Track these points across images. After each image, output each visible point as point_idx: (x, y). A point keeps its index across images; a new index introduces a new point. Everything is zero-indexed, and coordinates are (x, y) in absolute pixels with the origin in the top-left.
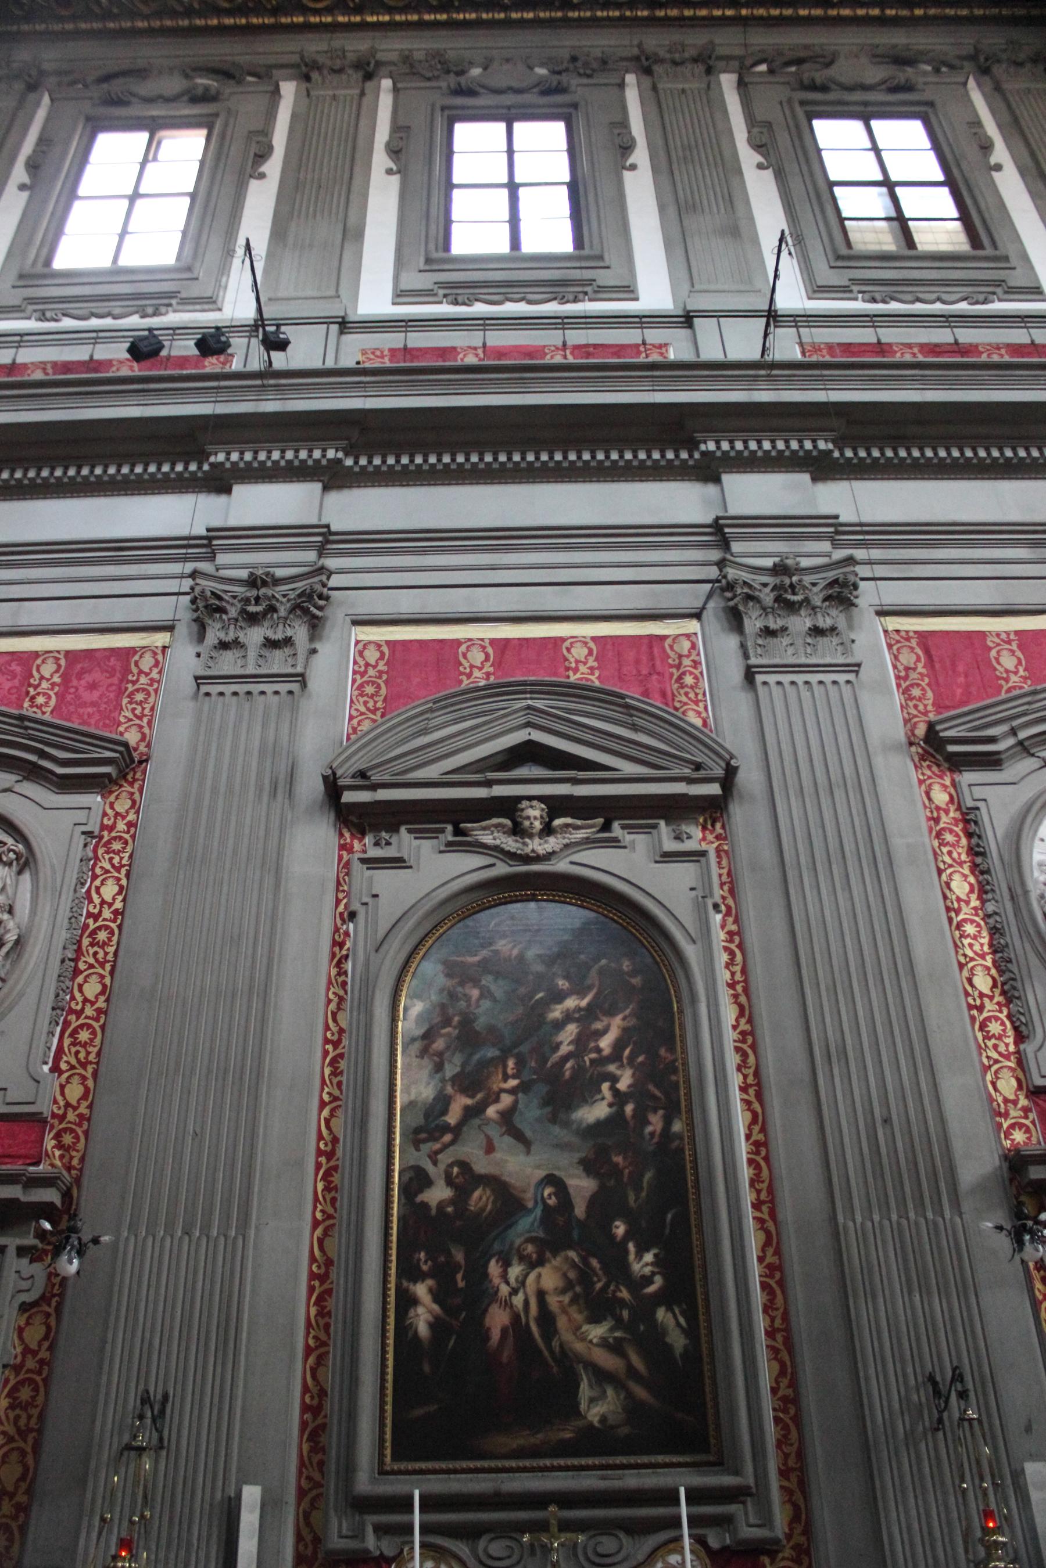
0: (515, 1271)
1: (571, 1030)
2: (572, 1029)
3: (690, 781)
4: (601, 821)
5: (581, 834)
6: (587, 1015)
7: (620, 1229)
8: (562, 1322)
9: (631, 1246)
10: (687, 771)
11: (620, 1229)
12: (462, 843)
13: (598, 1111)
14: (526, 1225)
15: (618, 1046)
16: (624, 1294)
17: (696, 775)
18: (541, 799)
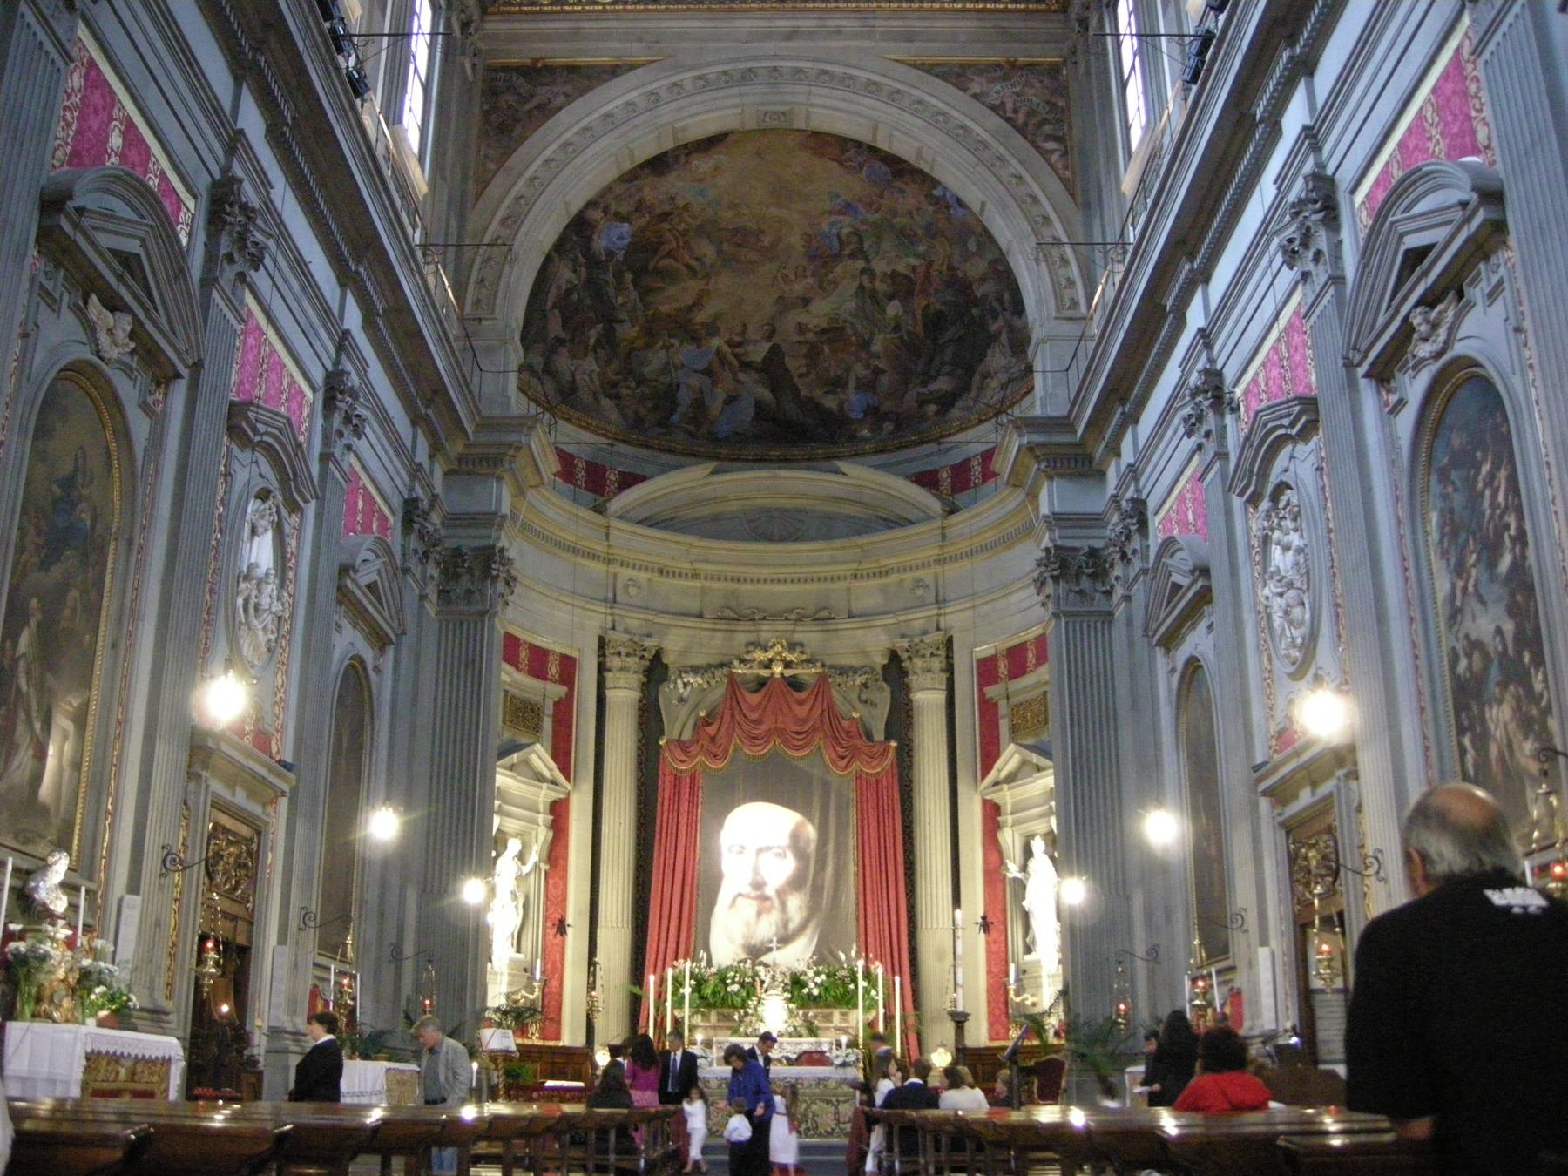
0: (1495, 711)
1: (1488, 493)
2: (1488, 493)
3: (1467, 220)
4: (1452, 294)
5: (1450, 314)
6: (1492, 476)
7: (1527, 658)
8: (1515, 746)
9: (1532, 671)
10: (1458, 215)
11: (1527, 658)
12: (1419, 365)
13: (1505, 562)
14: (1494, 673)
15: (1506, 498)
16: (1535, 712)
17: (1468, 212)
18: (1416, 306)
